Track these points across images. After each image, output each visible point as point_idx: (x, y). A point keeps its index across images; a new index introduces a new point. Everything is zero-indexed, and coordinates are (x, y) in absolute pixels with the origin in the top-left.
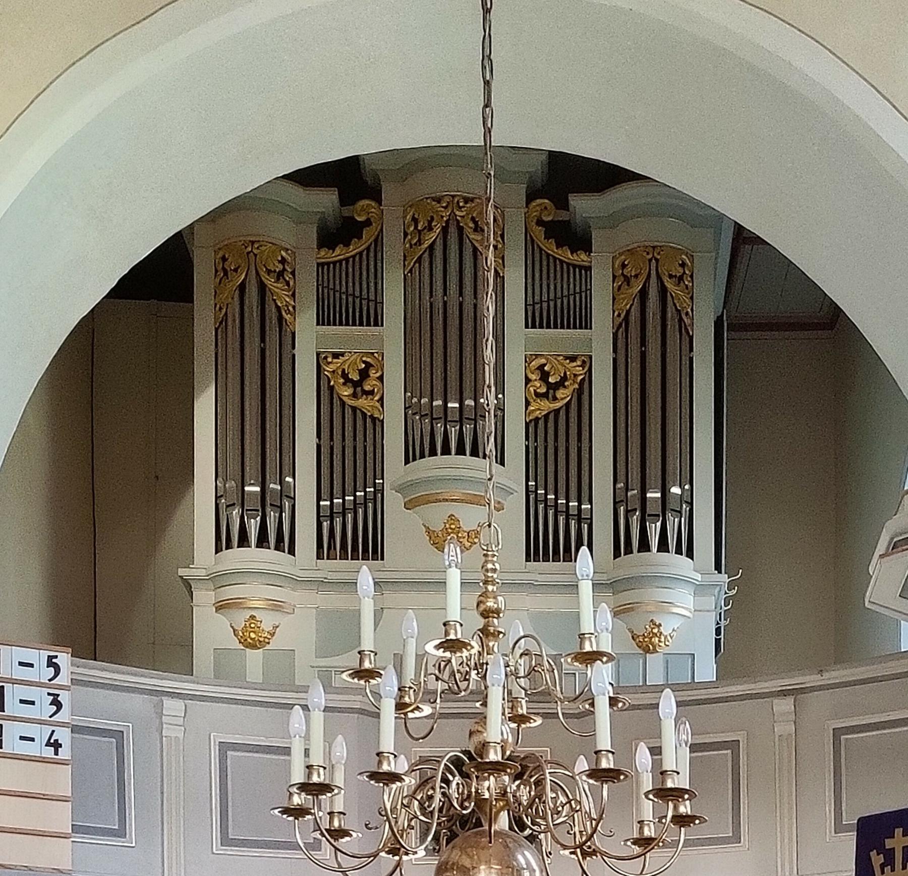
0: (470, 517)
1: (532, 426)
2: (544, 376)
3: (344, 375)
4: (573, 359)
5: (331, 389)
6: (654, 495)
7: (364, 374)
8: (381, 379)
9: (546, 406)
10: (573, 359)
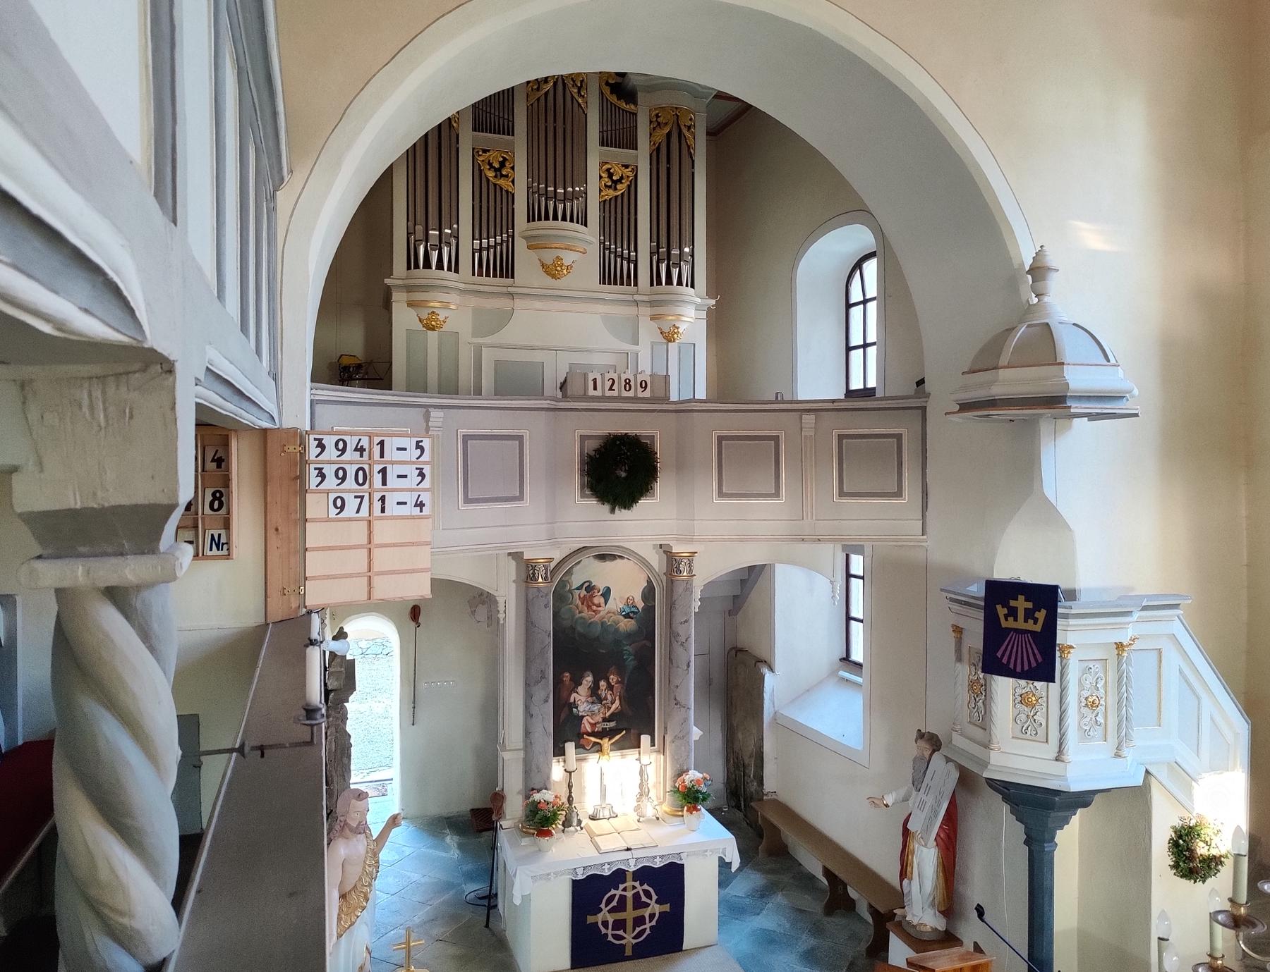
0: (568, 258)
1: (603, 204)
2: (610, 176)
3: (490, 164)
4: (627, 167)
5: (481, 171)
6: (675, 252)
7: (502, 164)
8: (513, 168)
9: (611, 193)
10: (627, 167)
